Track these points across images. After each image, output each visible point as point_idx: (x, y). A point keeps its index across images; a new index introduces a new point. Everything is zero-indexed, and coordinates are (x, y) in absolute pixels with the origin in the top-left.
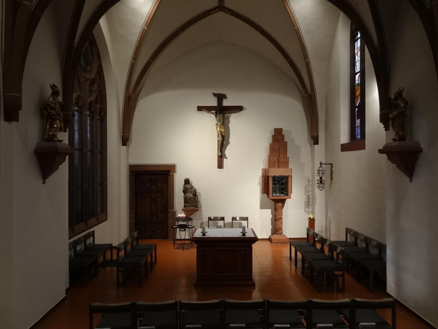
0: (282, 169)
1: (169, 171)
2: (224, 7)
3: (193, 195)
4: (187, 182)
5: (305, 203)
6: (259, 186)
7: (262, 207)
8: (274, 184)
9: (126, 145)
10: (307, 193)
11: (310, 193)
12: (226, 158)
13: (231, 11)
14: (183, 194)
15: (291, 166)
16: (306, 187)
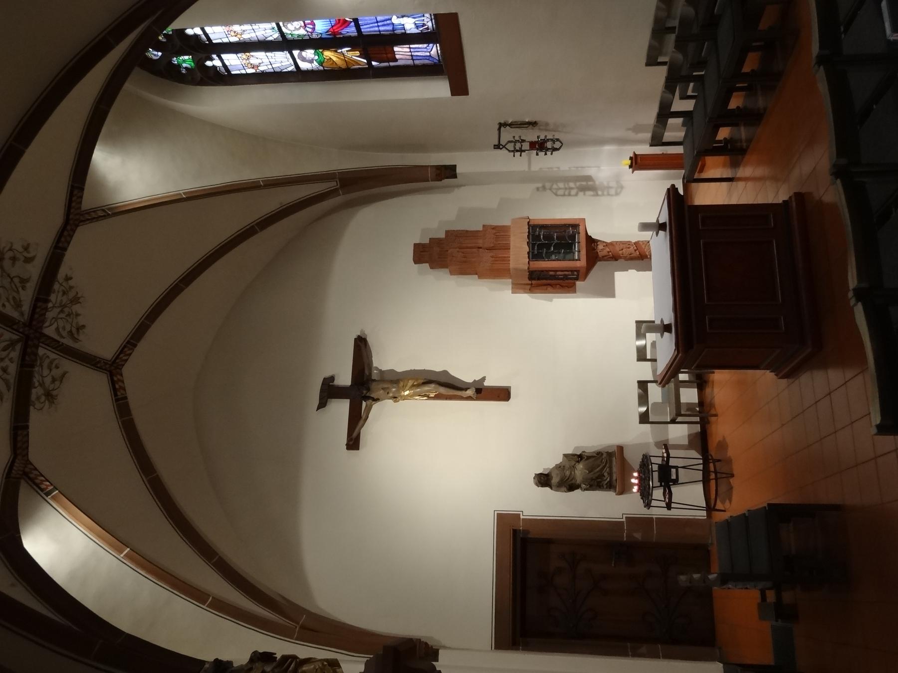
0: (512, 238)
1: (515, 532)
2: (114, 362)
3: (578, 462)
4: (543, 480)
5: (597, 195)
6: (554, 300)
7: (608, 291)
8: (548, 257)
9: (438, 650)
10: (573, 192)
12: (484, 379)
13: (125, 347)
14: (578, 492)
15: (507, 222)
16: (556, 195)
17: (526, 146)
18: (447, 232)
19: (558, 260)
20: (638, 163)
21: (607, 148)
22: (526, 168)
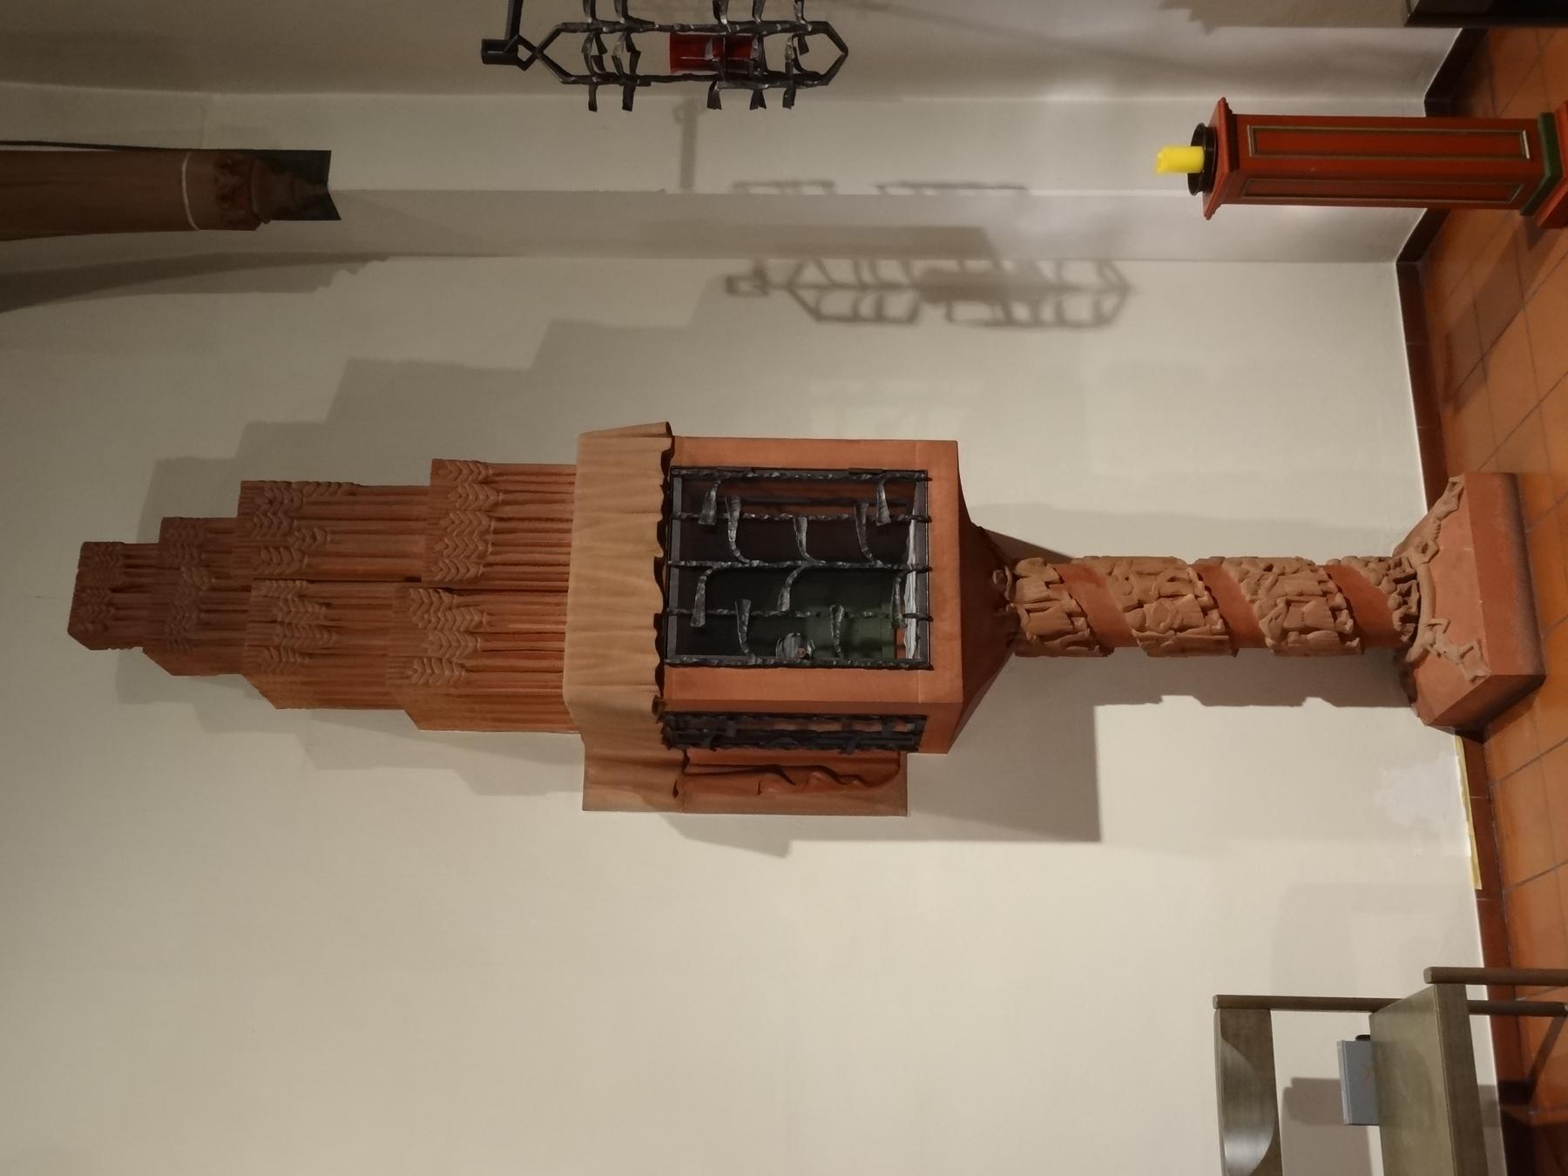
0: (578, 539)
5: (1009, 322)
6: (799, 847)
7: (1070, 811)
8: (764, 648)
10: (898, 304)
11: (890, 269)
15: (560, 452)
16: (817, 314)
17: (655, 52)
18: (251, 492)
19: (812, 662)
20: (1236, 162)
21: (1068, 98)
22: (673, 187)
